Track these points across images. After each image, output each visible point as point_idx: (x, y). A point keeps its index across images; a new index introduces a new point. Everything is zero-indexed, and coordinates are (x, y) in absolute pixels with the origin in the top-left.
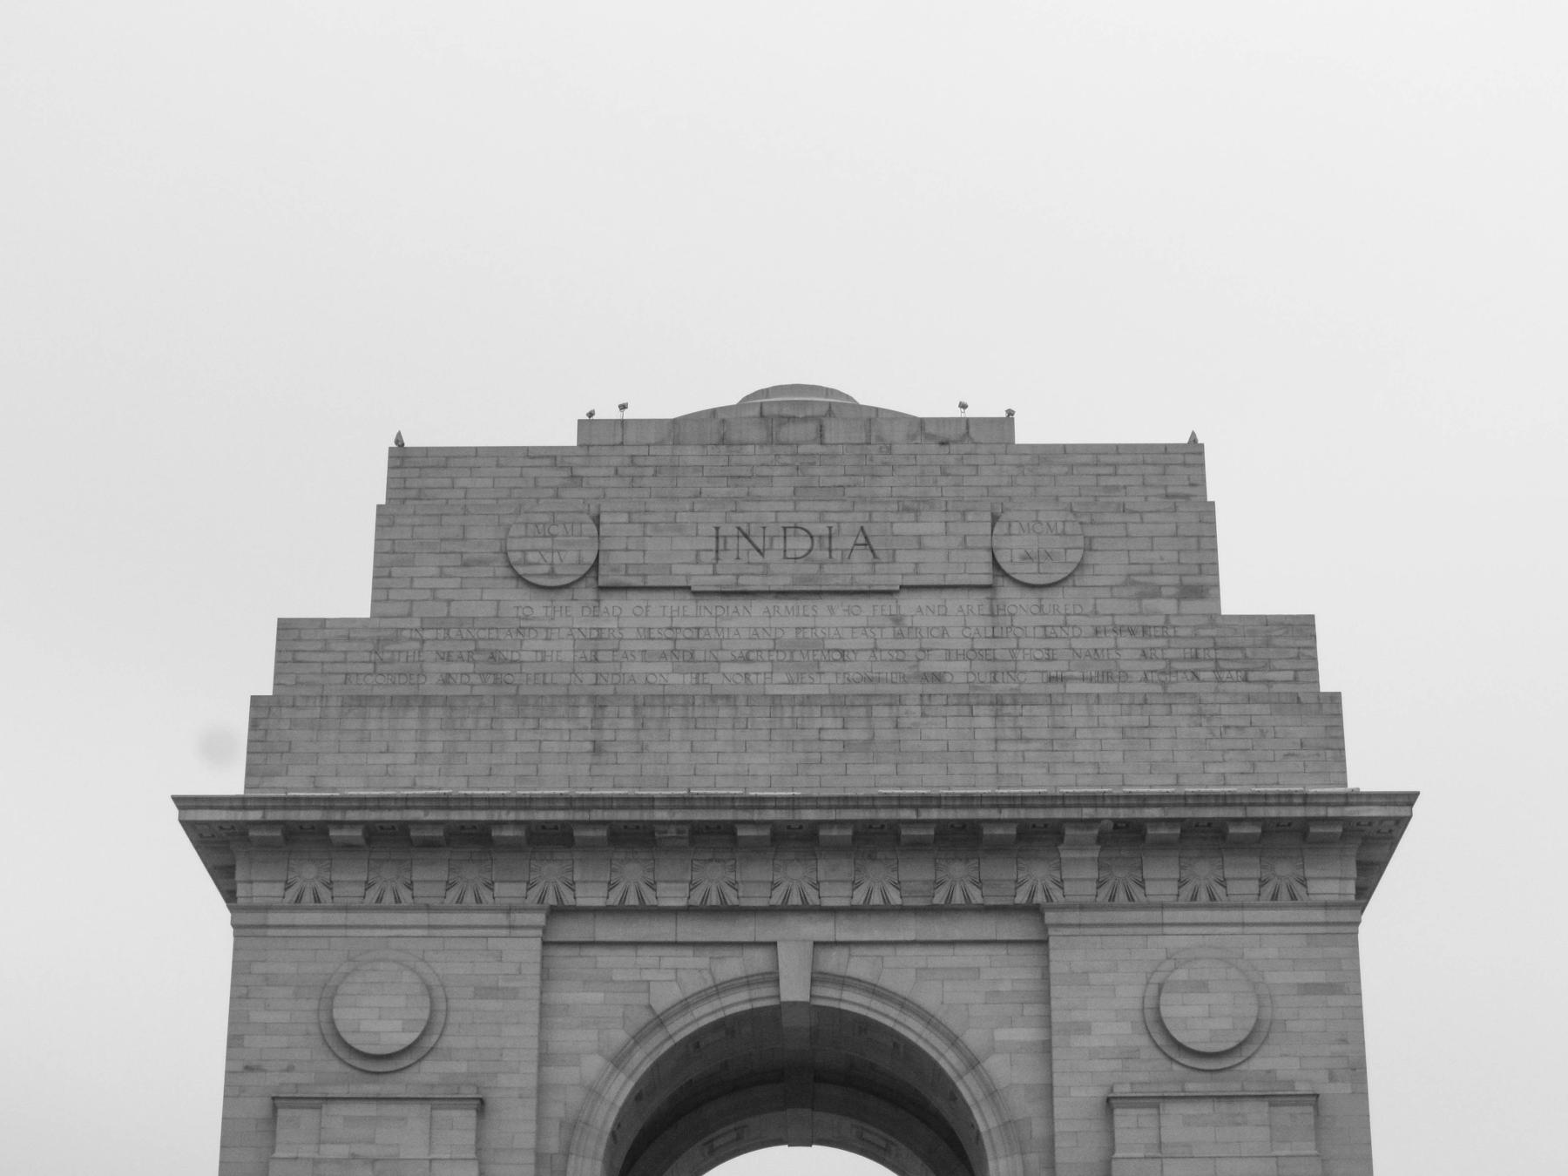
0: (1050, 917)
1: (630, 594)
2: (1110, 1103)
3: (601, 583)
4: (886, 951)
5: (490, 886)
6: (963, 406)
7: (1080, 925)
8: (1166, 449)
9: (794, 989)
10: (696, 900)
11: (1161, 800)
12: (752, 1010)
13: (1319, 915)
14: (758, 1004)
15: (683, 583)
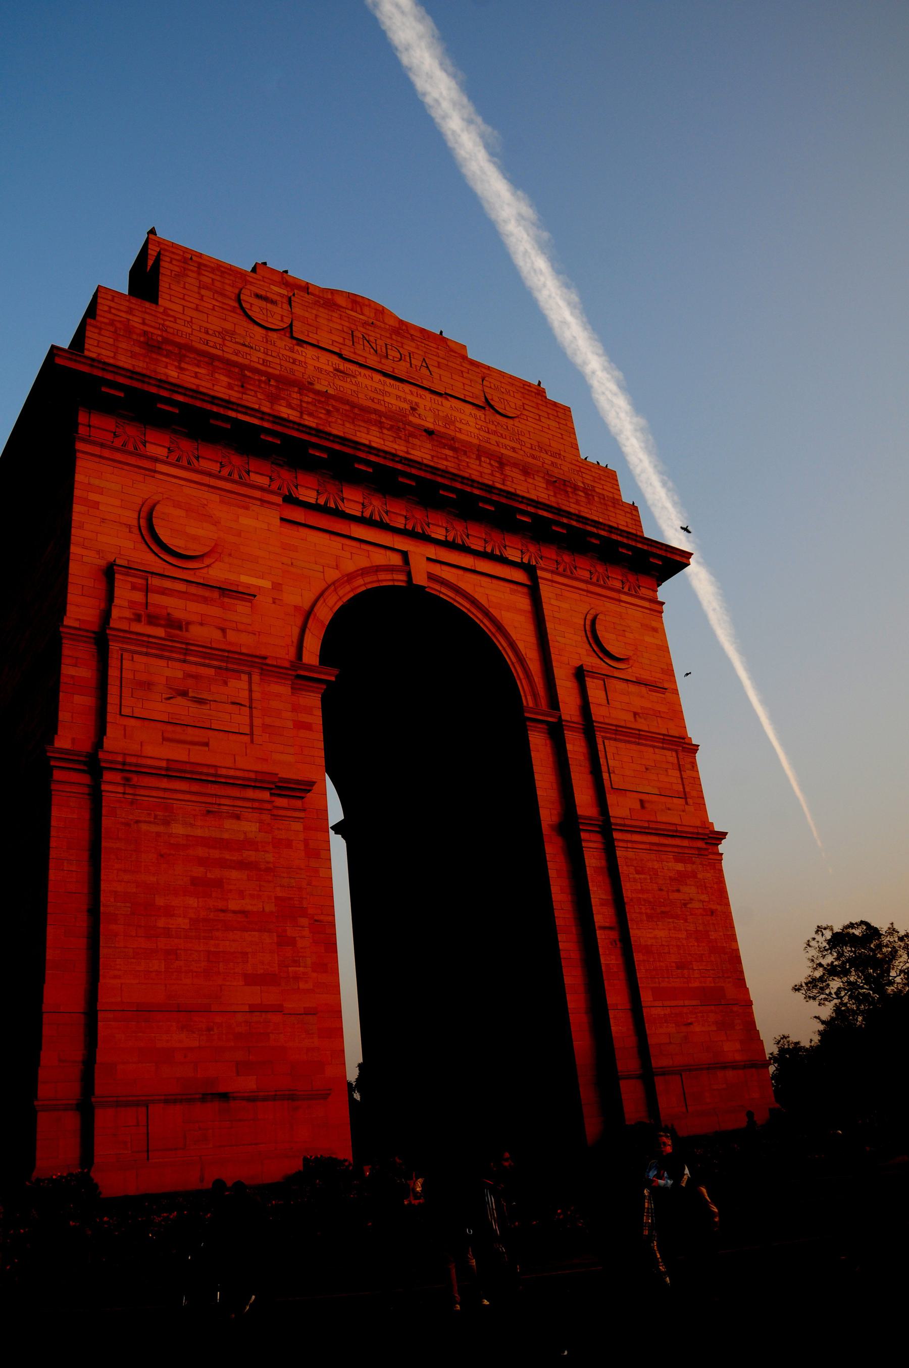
0: (540, 573)
1: (309, 348)
2: (580, 674)
3: (295, 335)
4: (460, 572)
5: (248, 472)
6: (441, 332)
7: (552, 581)
8: (530, 385)
9: (420, 579)
10: (367, 514)
11: (596, 524)
12: (394, 586)
13: (647, 604)
14: (396, 584)
15: (337, 350)
